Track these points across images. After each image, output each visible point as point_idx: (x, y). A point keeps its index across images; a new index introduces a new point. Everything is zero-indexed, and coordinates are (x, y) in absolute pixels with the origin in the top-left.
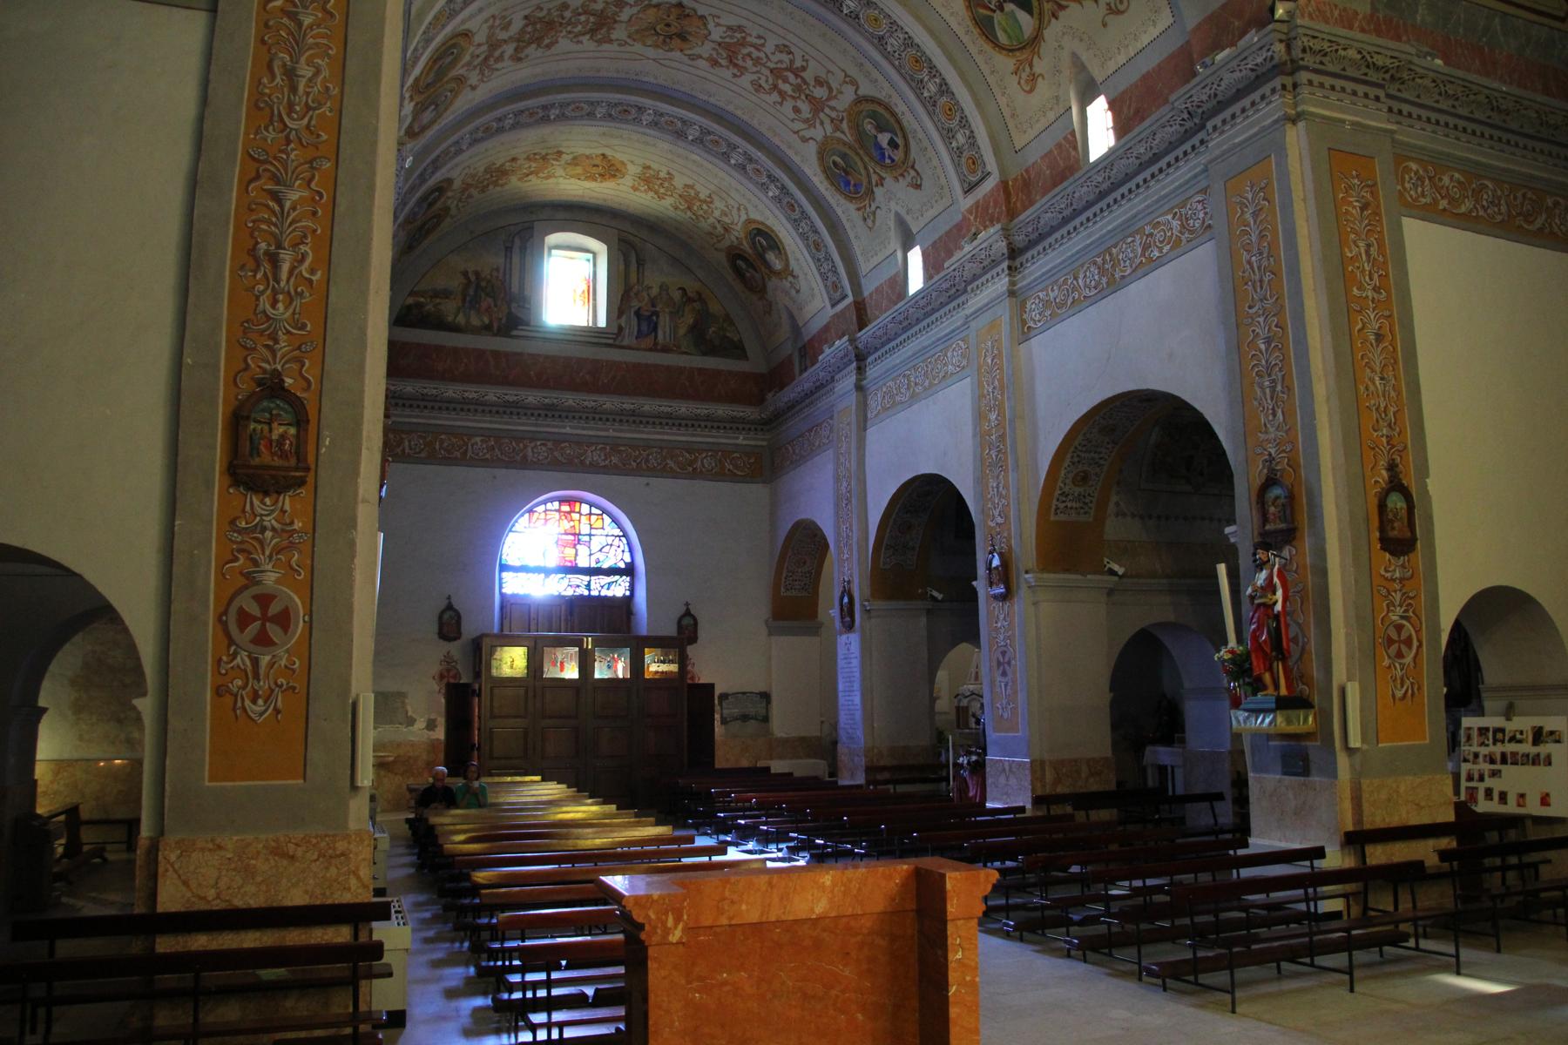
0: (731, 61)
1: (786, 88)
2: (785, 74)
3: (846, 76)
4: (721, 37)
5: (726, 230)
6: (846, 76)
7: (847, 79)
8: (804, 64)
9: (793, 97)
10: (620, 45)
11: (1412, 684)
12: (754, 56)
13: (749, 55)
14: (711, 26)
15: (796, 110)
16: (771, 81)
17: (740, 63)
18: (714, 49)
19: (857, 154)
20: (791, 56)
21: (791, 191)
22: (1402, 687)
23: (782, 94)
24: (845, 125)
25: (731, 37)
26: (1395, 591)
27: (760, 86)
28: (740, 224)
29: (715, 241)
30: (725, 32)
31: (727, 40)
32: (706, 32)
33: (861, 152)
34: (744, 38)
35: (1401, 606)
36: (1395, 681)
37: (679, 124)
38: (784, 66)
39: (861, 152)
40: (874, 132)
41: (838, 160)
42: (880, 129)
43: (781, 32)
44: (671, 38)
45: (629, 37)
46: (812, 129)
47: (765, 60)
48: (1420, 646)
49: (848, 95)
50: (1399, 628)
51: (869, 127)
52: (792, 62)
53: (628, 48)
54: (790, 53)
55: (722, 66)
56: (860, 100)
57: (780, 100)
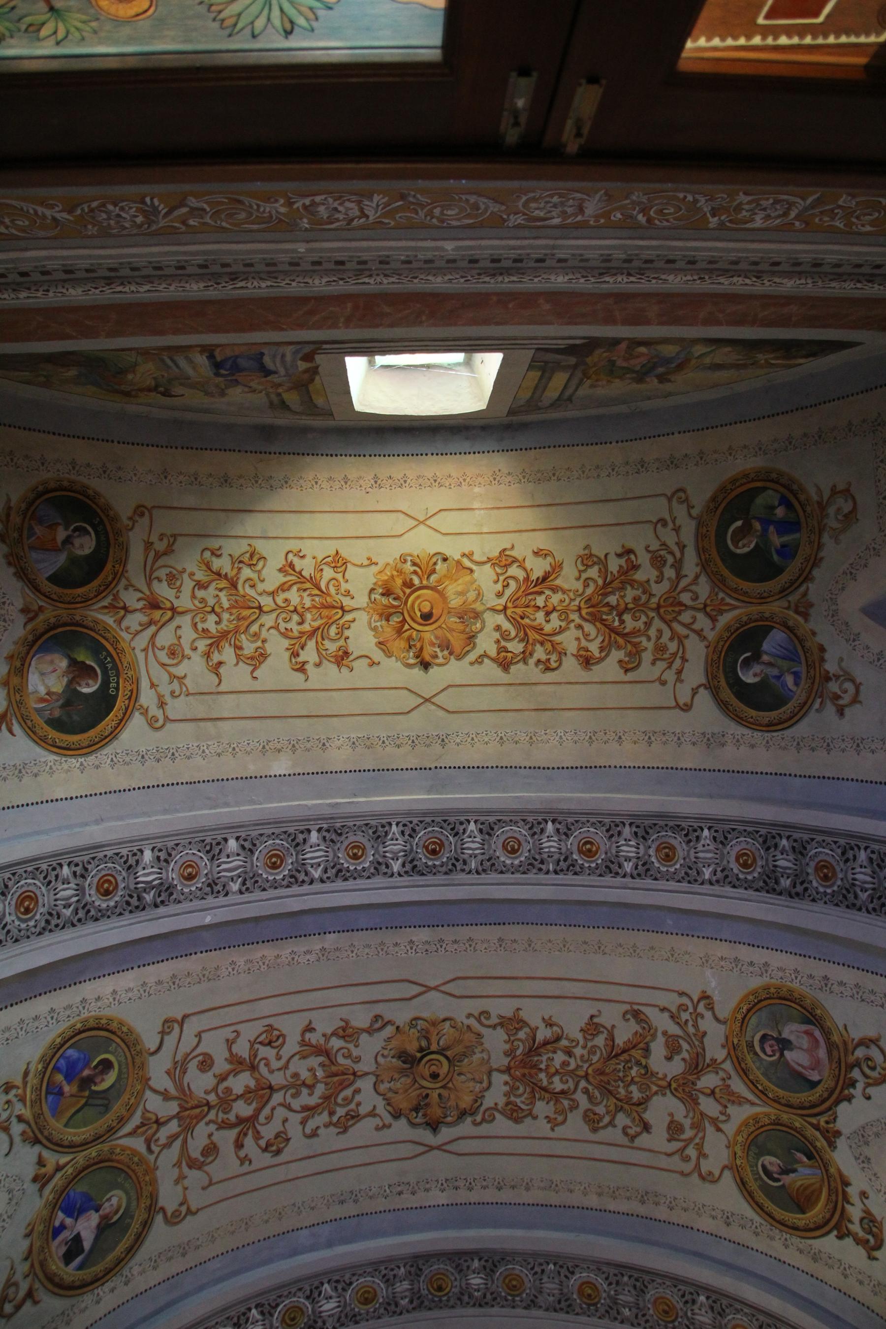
0: (327, 1053)
1: (240, 1083)
2: (254, 1105)
3: (189, 1212)
4: (357, 1091)
5: (154, 604)
6: (189, 1212)
7: (184, 1209)
8: (242, 1154)
9: (223, 1078)
10: (486, 1013)
12: (305, 1091)
13: (311, 1087)
14: (380, 1103)
15: (206, 1063)
16: (263, 1069)
17: (315, 1061)
18: (358, 1060)
19: (97, 1138)
20: (263, 1143)
21: (127, 919)
23: (238, 1064)
24: (138, 1144)
25: (348, 1101)
27: (269, 1044)
28: (141, 656)
29: (154, 538)
30: (359, 1104)
31: (348, 1092)
32: (383, 1087)
33: (93, 1152)
34: (332, 1113)
37: (346, 862)
38: (262, 1119)
39: (93, 1152)
40: (106, 1208)
41: (110, 1078)
42: (103, 1228)
43: (296, 1169)
44: (421, 1050)
45: (479, 1035)
46: (169, 1065)
47: (289, 1099)
49: (169, 1197)
51: (115, 1200)
52: (258, 1136)
53: (475, 1006)
54: (265, 1150)
55: (334, 1034)
56: (153, 1208)
57: (235, 1049)
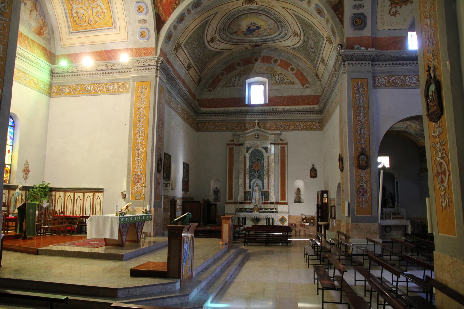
11: (448, 198)
22: (445, 201)
26: (437, 143)
35: (440, 151)
36: (442, 197)
48: (449, 175)
50: (441, 164)
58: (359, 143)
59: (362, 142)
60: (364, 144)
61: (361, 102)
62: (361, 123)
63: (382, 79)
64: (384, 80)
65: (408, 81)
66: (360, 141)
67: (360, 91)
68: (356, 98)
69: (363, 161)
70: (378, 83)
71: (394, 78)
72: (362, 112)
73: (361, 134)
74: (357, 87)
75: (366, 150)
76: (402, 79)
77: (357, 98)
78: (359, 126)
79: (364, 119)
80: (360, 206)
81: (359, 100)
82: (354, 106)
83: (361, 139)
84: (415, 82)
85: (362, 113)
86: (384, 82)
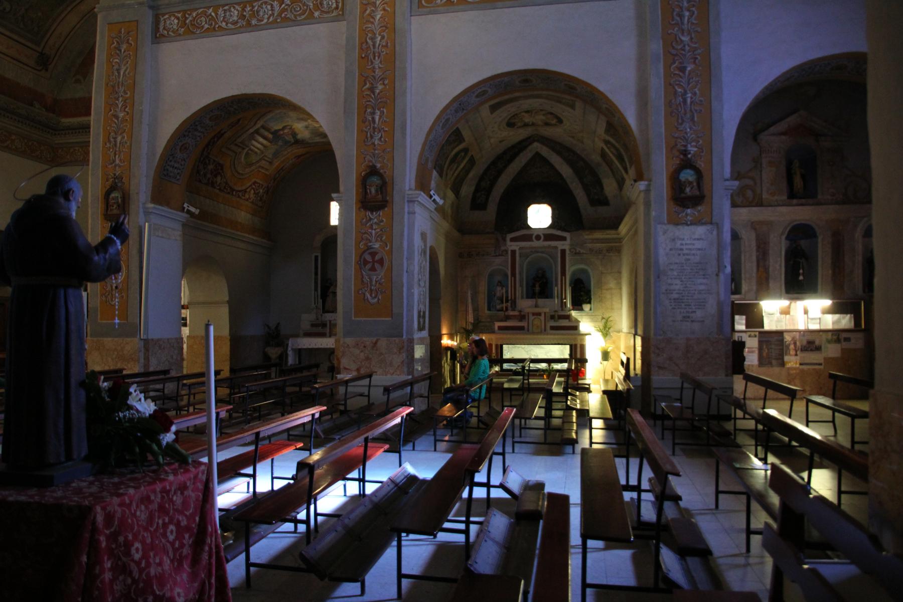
58: (110, 166)
59: (117, 162)
60: (120, 166)
61: (122, 74)
62: (118, 120)
63: (173, 18)
64: (176, 21)
65: (222, 19)
66: (114, 161)
67: (123, 51)
68: (113, 66)
69: (114, 203)
70: (164, 29)
71: (194, 15)
72: (122, 96)
73: (116, 145)
74: (117, 42)
75: (123, 180)
76: (210, 15)
77: (116, 67)
78: (114, 127)
79: (125, 111)
80: (106, 302)
81: (118, 70)
82: (107, 85)
83: (115, 157)
84: (235, 18)
85: (121, 99)
86: (175, 27)
